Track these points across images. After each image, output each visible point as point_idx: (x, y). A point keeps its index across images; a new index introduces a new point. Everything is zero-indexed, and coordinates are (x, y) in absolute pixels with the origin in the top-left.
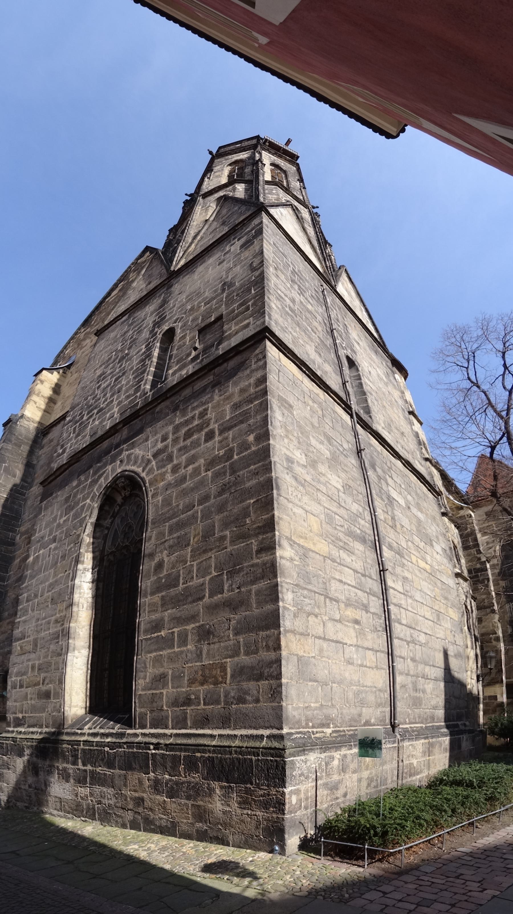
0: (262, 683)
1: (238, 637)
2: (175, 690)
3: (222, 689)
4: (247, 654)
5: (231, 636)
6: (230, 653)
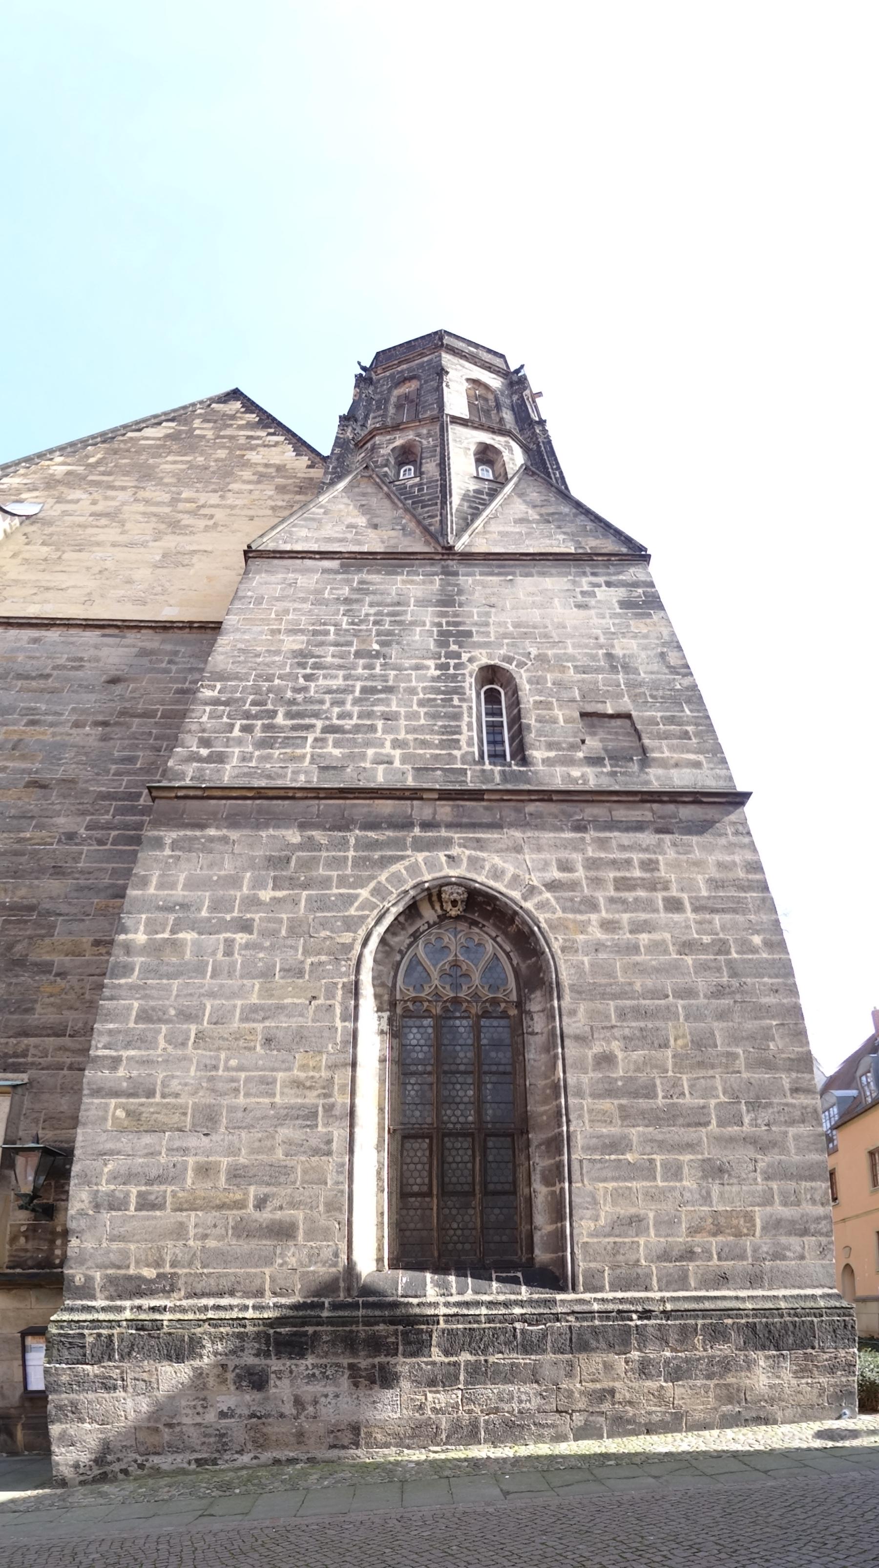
0: (806, 1239)
1: (770, 1183)
2: (662, 1240)
3: (748, 1243)
4: (785, 1204)
5: (759, 1180)
6: (758, 1200)
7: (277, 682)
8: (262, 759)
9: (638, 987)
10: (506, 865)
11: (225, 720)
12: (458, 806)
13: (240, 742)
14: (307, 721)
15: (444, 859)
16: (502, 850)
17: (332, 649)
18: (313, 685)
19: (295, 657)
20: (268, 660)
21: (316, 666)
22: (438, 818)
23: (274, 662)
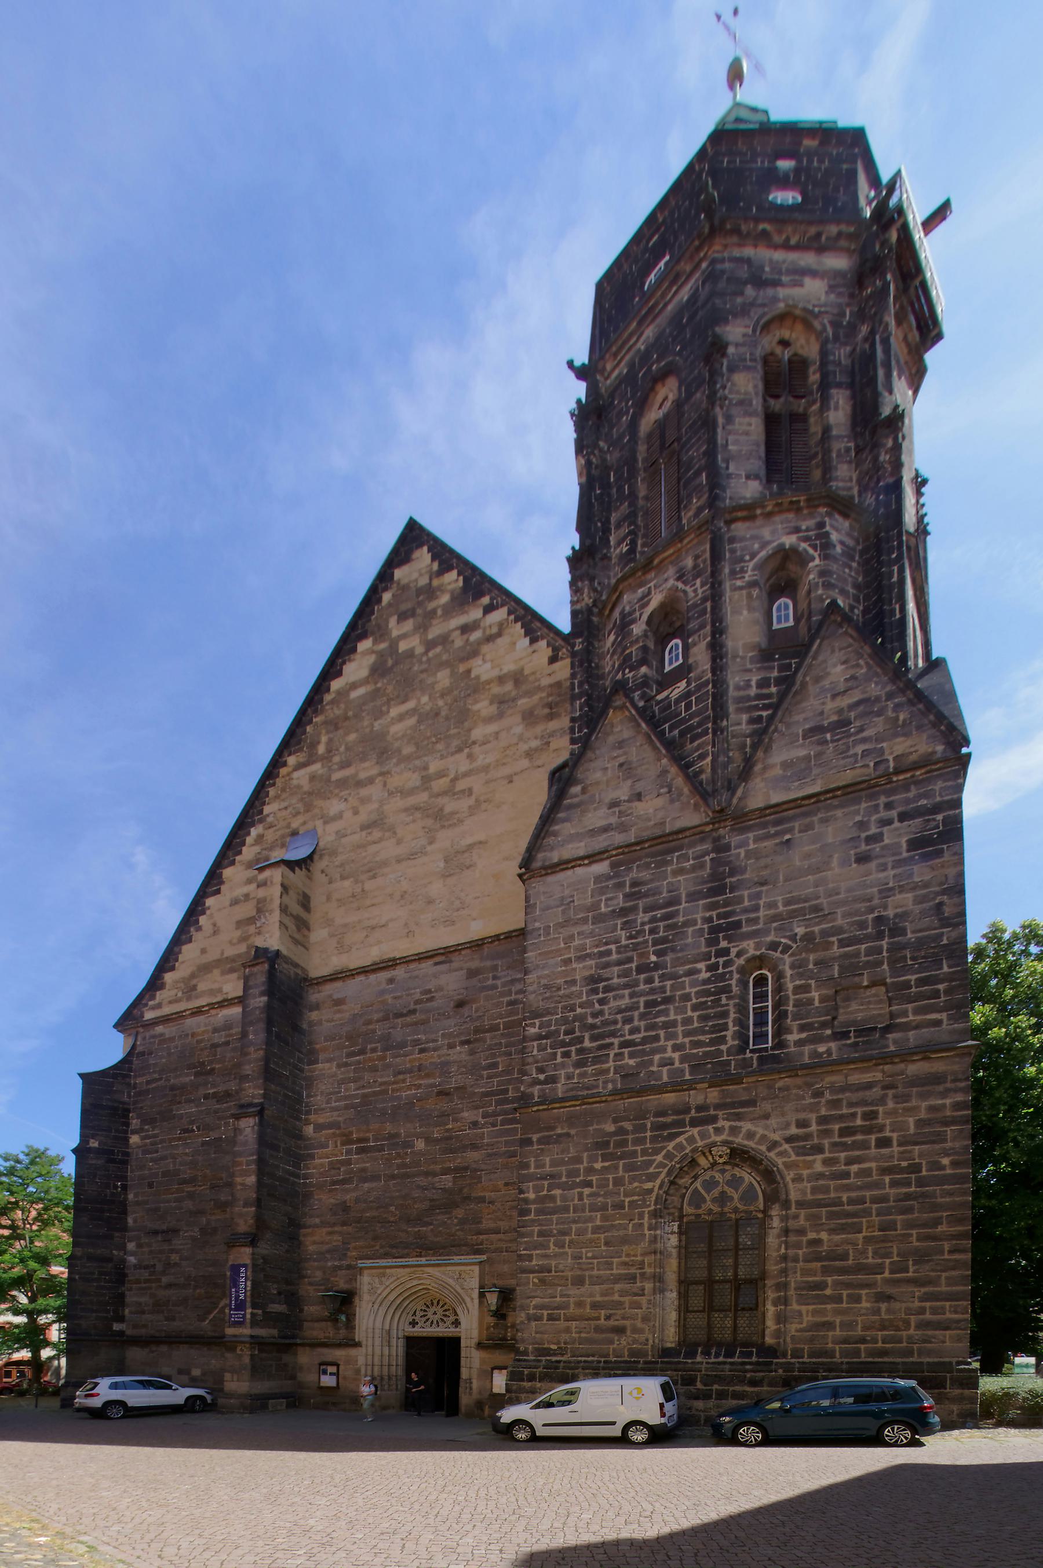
7: (579, 1010)
8: (582, 1075)
9: (844, 1199)
10: (757, 1129)
11: (549, 1051)
12: (723, 1090)
13: (563, 1065)
14: (608, 1041)
15: (712, 1131)
16: (754, 1119)
17: (616, 969)
18: (606, 1007)
19: (588, 985)
20: (567, 992)
21: (607, 989)
22: (708, 1101)
23: (572, 993)
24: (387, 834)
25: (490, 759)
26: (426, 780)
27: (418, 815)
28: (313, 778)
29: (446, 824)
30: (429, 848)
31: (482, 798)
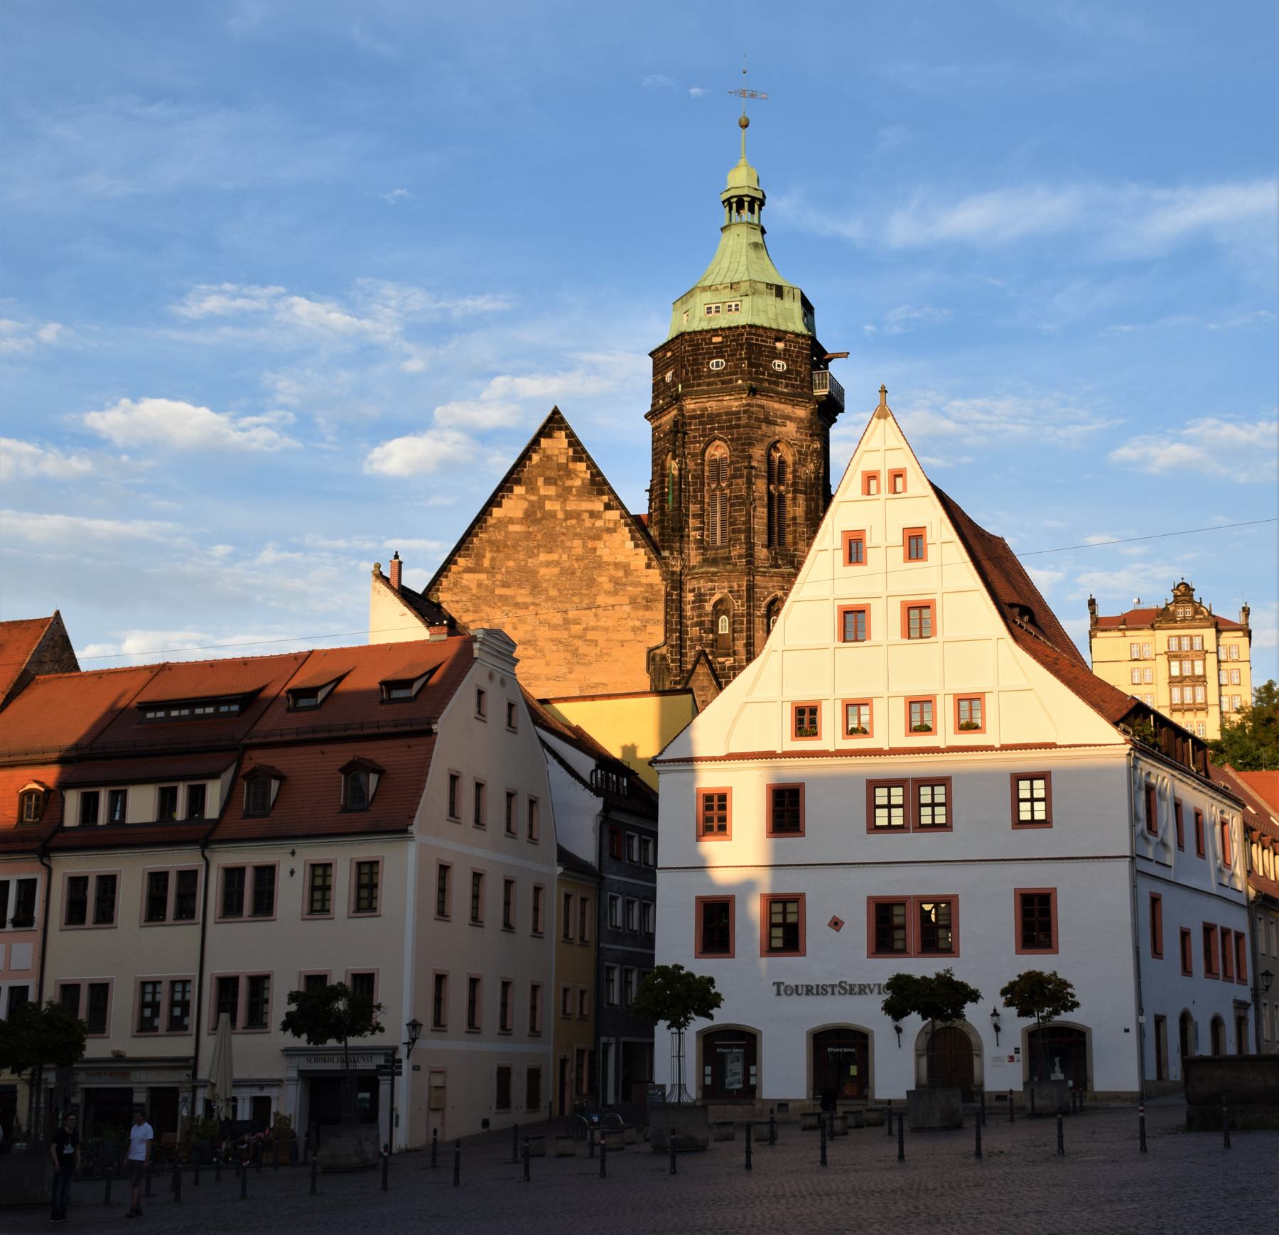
24: (539, 654)
25: (610, 623)
26: (567, 622)
27: (560, 647)
28: (480, 585)
29: (580, 661)
30: (569, 676)
31: (604, 651)
